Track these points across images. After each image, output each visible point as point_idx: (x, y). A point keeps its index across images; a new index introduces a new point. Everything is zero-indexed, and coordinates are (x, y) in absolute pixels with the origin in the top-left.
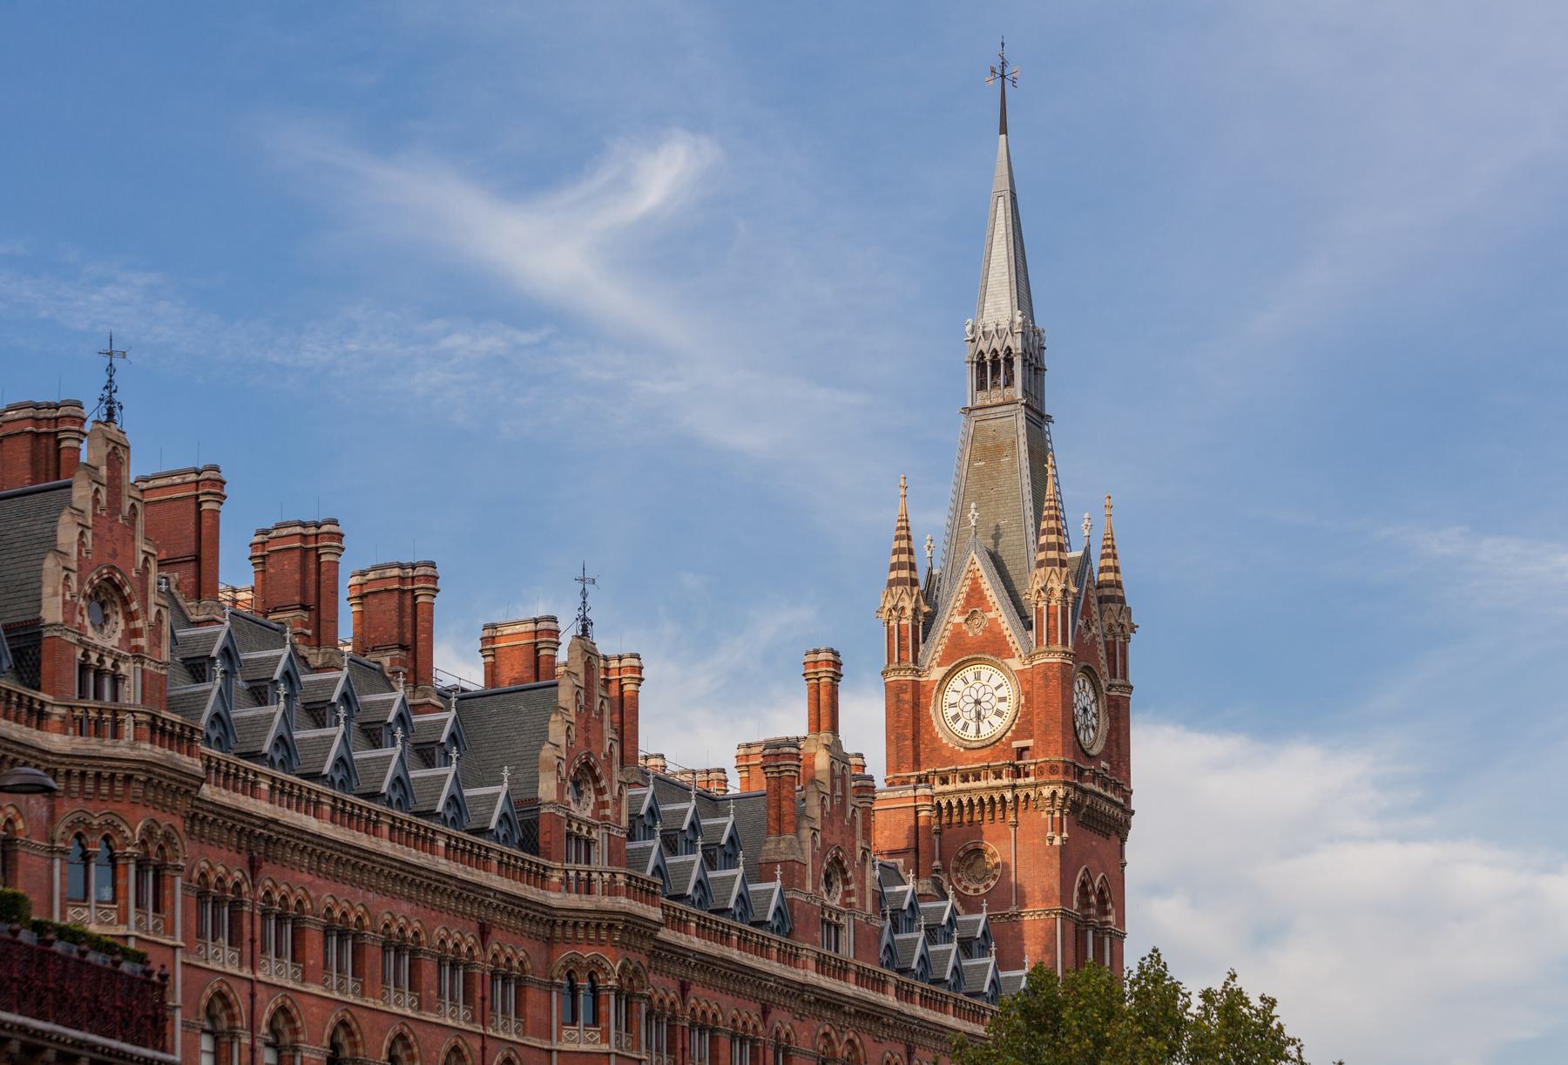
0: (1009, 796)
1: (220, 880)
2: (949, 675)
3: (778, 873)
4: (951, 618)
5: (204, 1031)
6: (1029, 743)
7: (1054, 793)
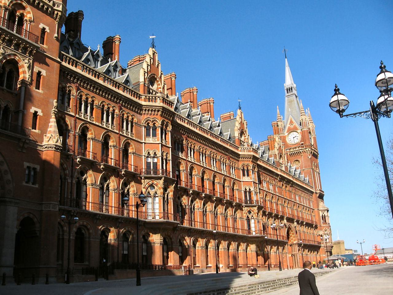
0: (301, 151)
1: (179, 139)
2: (289, 134)
3: (273, 156)
4: (288, 125)
5: (177, 170)
6: (303, 143)
7: (308, 150)
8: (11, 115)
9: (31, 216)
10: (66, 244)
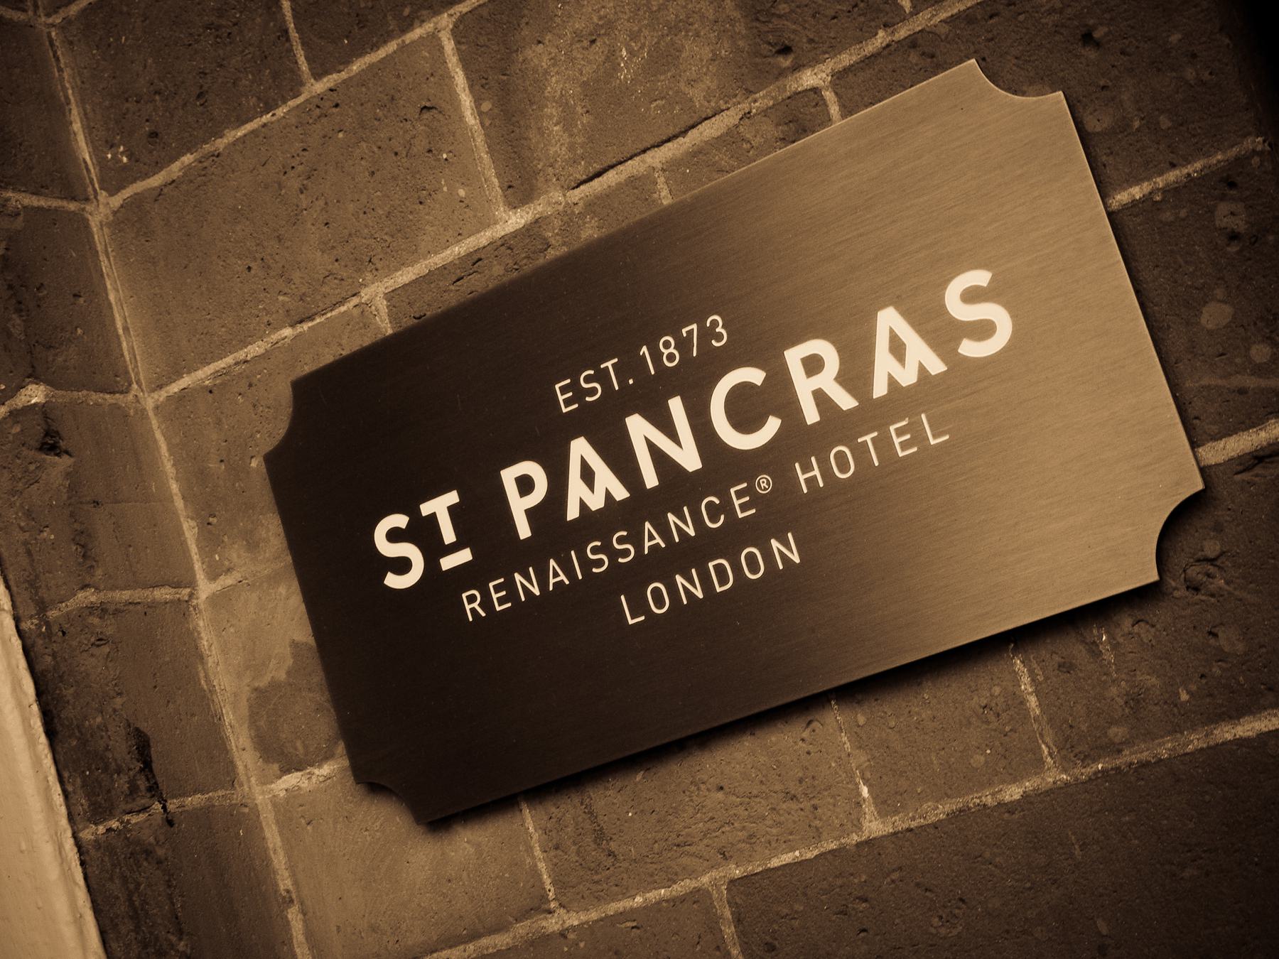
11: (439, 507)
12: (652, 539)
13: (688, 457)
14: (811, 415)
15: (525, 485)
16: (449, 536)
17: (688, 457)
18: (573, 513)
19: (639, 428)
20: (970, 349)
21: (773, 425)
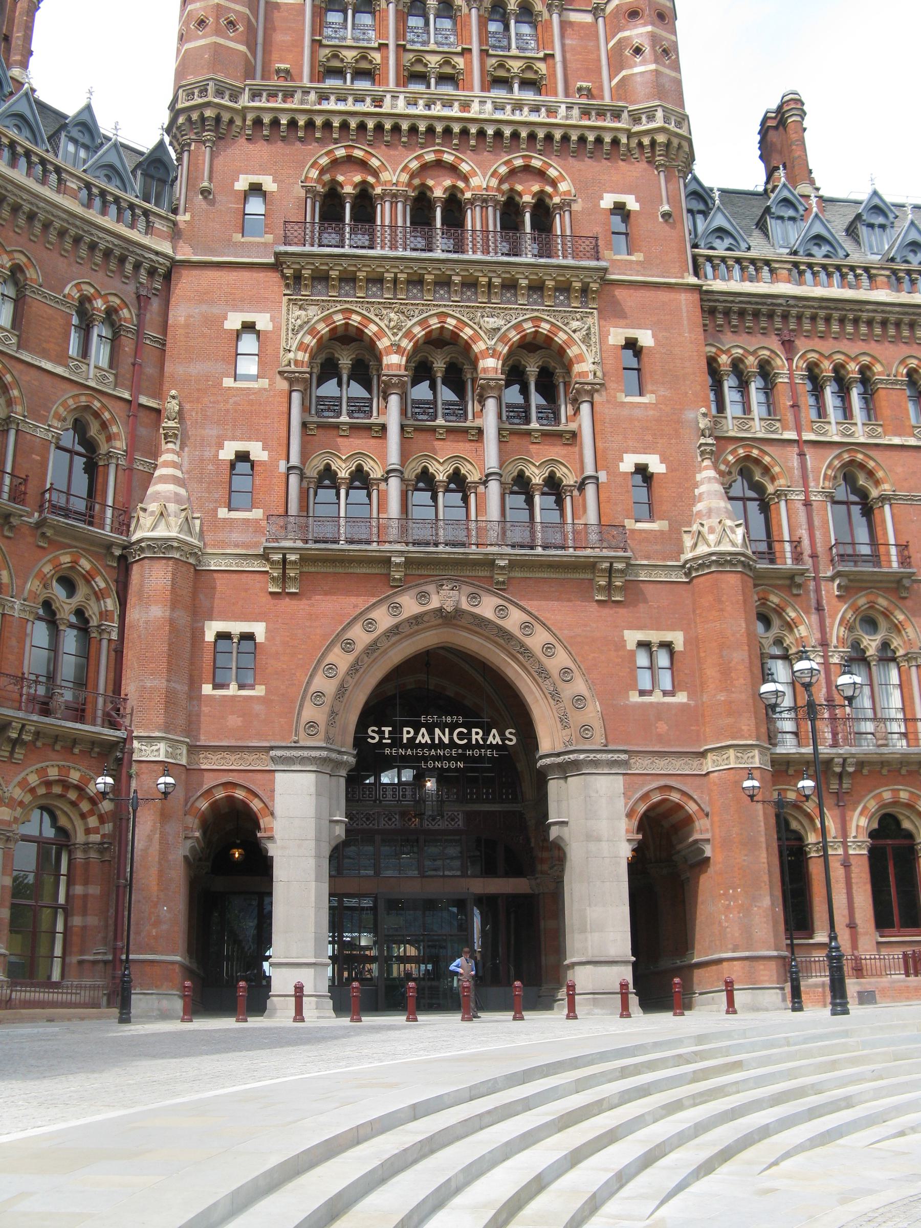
8: (568, 499)
9: (675, 797)
10: (837, 872)
11: (387, 730)
12: (433, 752)
13: (446, 741)
14: (474, 742)
15: (408, 732)
16: (387, 736)
17: (446, 741)
18: (417, 742)
19: (437, 731)
20: (507, 742)
21: (466, 741)
